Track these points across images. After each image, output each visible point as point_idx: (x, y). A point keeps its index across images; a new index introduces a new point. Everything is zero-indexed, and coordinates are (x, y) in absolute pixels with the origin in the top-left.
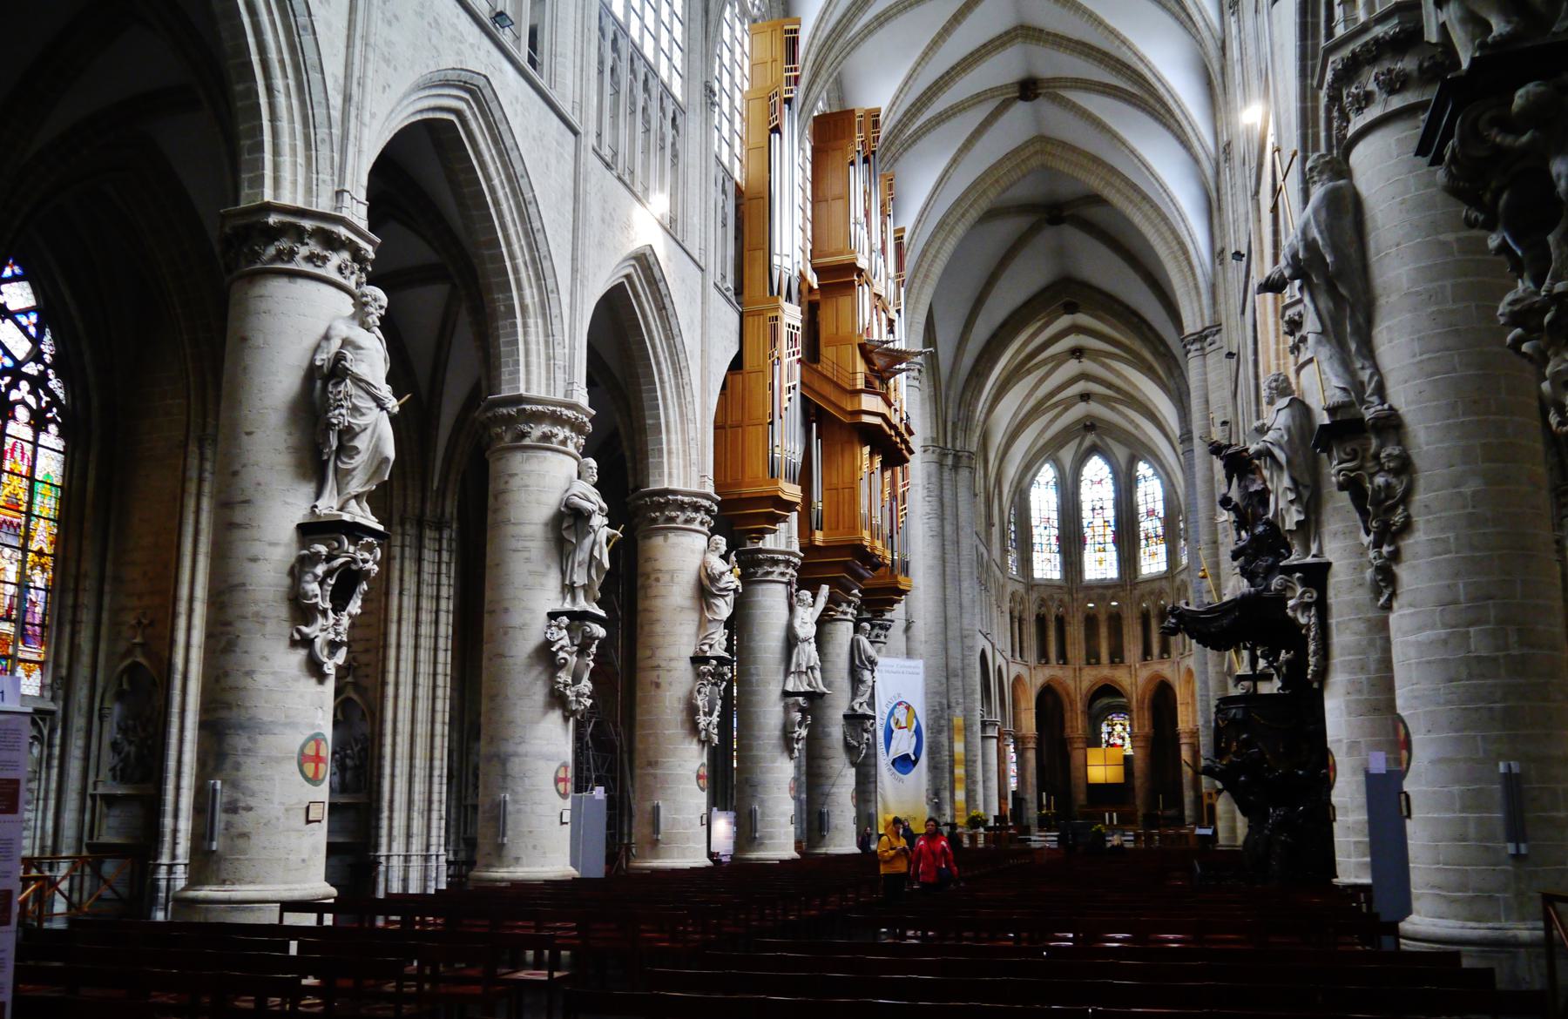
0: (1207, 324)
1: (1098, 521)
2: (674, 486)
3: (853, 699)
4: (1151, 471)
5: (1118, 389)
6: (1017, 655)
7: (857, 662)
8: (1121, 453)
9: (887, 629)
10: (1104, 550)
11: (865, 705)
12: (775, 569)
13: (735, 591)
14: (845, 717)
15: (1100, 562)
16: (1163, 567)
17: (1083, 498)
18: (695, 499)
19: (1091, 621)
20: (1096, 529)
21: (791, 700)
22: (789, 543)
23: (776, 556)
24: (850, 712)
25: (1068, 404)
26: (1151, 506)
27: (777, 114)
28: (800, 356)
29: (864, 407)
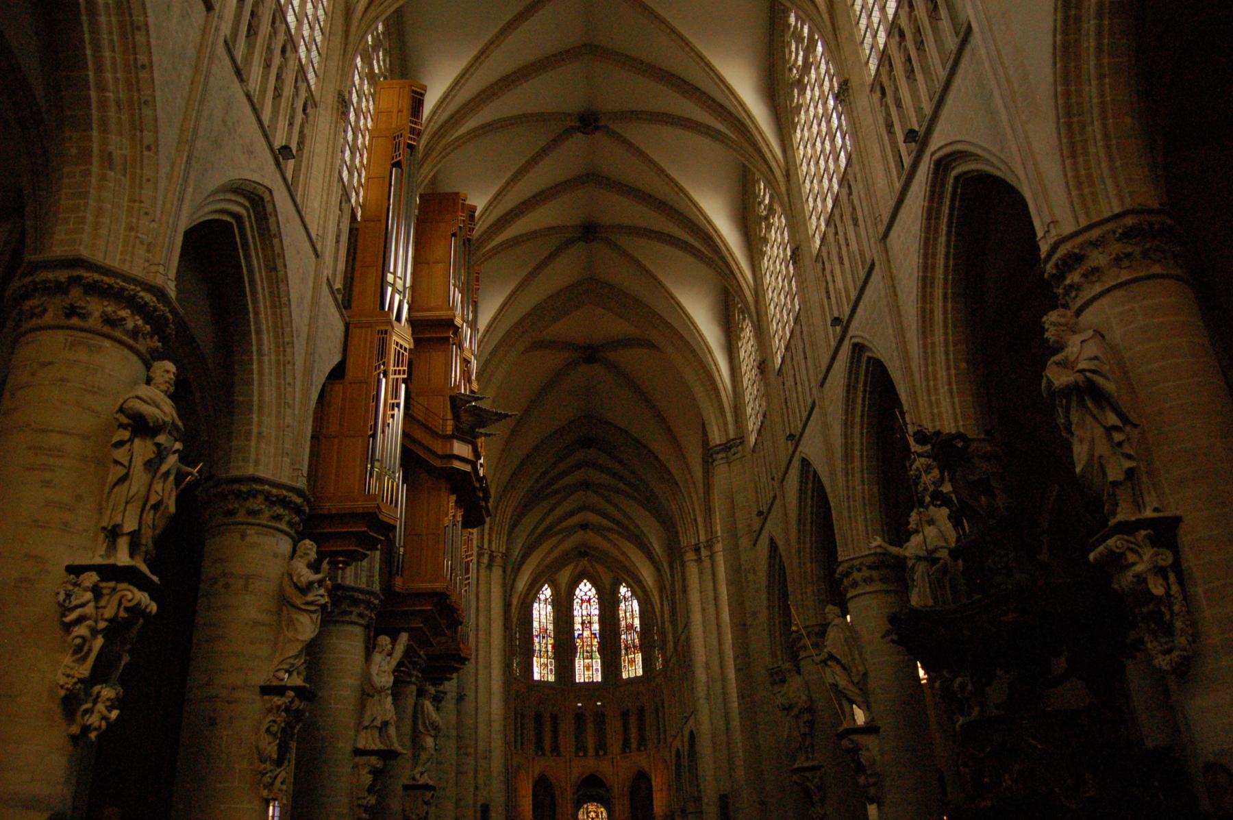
0: (732, 436)
1: (586, 633)
2: (262, 473)
3: (414, 766)
4: (629, 594)
5: (612, 520)
6: (519, 747)
7: (421, 728)
8: (607, 579)
9: (440, 701)
10: (592, 658)
11: (426, 774)
12: (353, 609)
13: (323, 607)
14: (406, 787)
15: (588, 670)
16: (640, 672)
17: (575, 613)
18: (285, 492)
19: (579, 717)
20: (585, 640)
21: (365, 759)
22: (370, 582)
23: (356, 594)
24: (411, 782)
25: (570, 531)
26: (630, 621)
27: (401, 151)
28: (405, 376)
29: (456, 452)
